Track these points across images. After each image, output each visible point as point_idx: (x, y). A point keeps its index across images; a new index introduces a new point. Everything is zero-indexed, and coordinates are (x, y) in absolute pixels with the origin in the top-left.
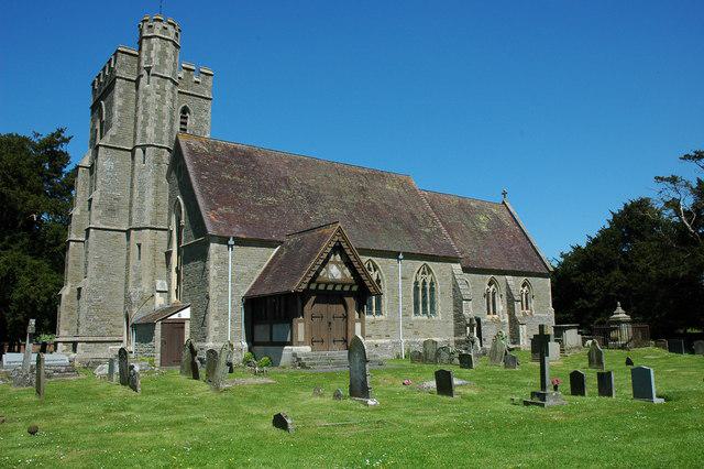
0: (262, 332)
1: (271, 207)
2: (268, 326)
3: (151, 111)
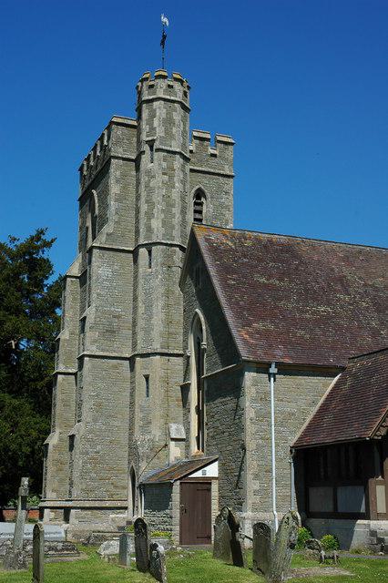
0: (320, 499)
1: (324, 321)
3: (157, 198)
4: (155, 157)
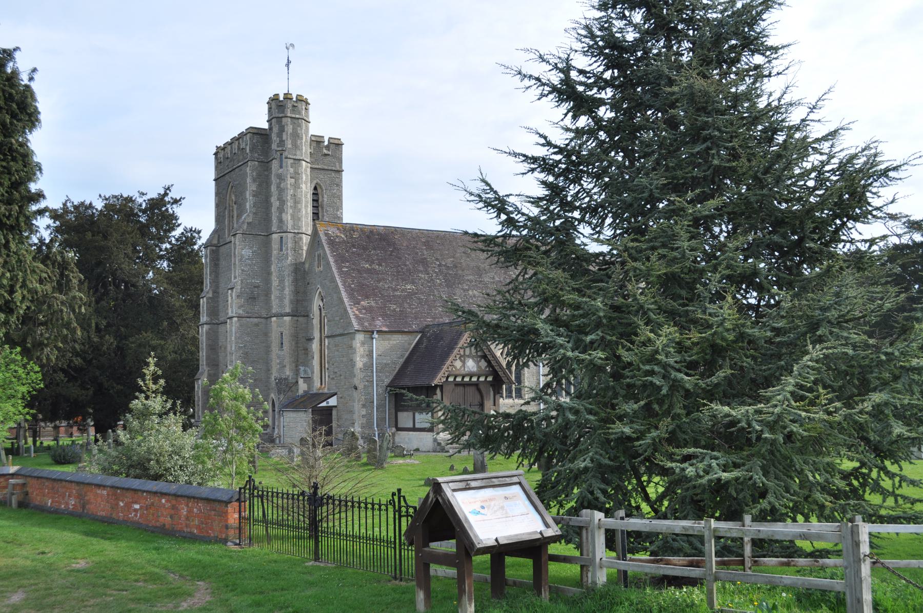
2: (411, 414)
4: (284, 164)
